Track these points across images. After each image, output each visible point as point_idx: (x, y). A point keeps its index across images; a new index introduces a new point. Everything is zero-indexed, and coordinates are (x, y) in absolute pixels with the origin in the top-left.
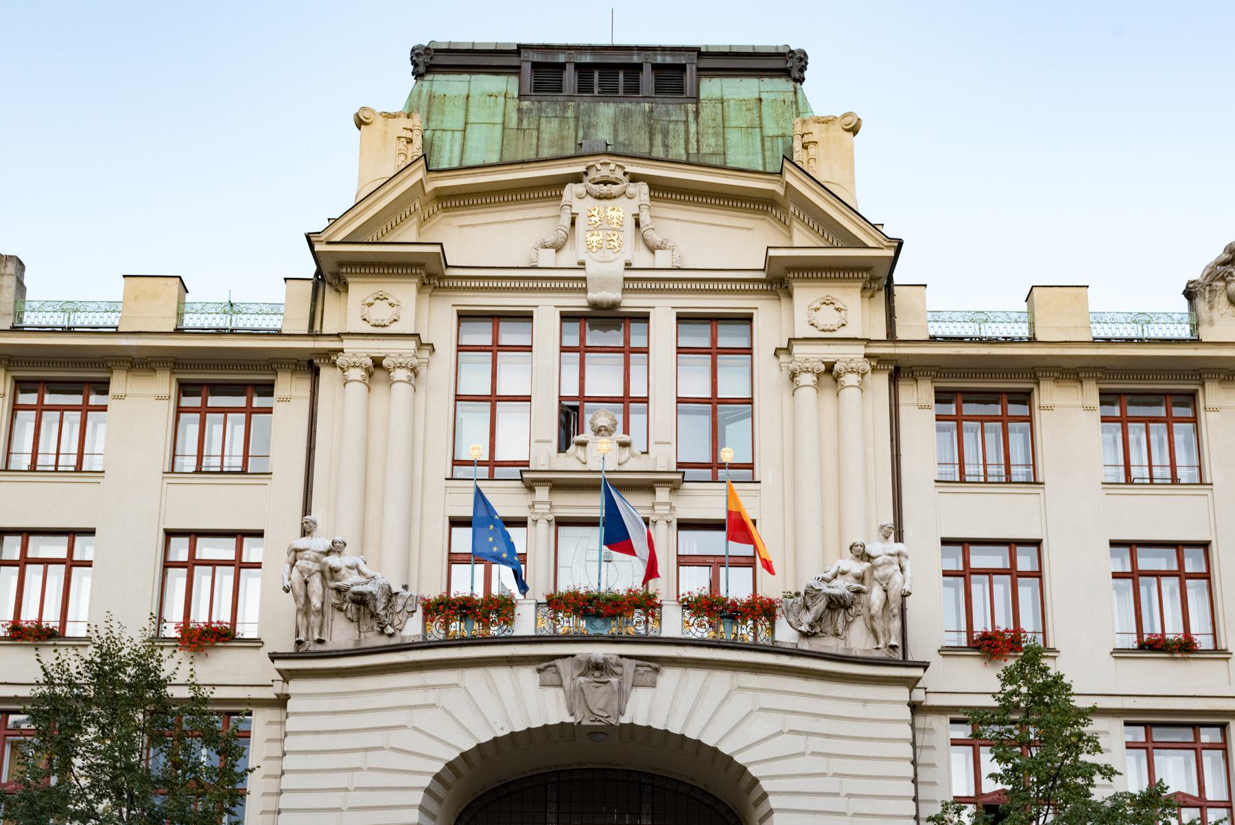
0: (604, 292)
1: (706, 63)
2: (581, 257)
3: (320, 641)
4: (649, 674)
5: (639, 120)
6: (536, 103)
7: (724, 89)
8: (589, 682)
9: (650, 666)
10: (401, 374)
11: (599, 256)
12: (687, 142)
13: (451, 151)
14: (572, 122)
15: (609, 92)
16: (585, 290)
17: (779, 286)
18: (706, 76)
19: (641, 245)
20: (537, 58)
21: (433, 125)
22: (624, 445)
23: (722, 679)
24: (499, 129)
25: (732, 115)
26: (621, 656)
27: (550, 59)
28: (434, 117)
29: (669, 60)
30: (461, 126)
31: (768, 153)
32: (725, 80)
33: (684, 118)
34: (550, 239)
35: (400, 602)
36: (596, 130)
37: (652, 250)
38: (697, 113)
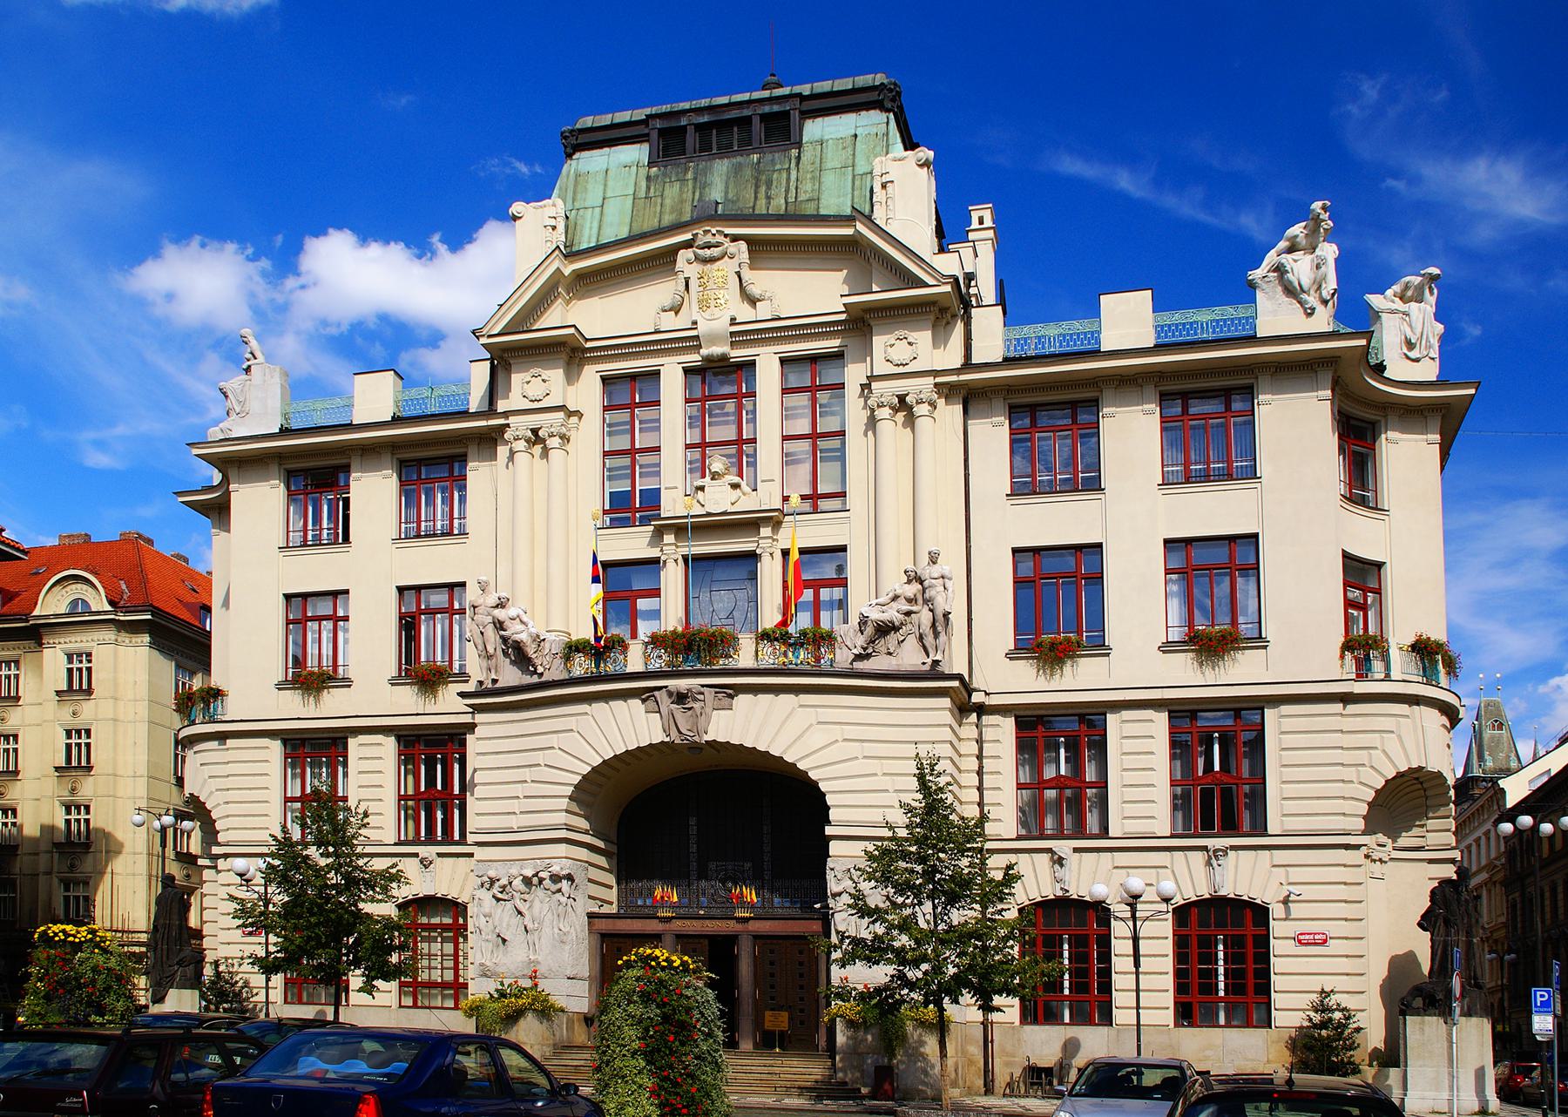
0: (714, 348)
1: (807, 106)
5: (748, 172)
6: (662, 168)
7: (826, 129)
11: (706, 315)
12: (787, 191)
13: (591, 228)
14: (690, 183)
15: (725, 151)
18: (809, 118)
21: (577, 205)
24: (630, 200)
25: (829, 155)
26: (703, 686)
27: (674, 124)
28: (579, 196)
29: (776, 108)
30: (600, 202)
31: (856, 193)
32: (826, 119)
33: (787, 166)
34: (667, 303)
36: (710, 189)
37: (753, 301)
38: (799, 158)
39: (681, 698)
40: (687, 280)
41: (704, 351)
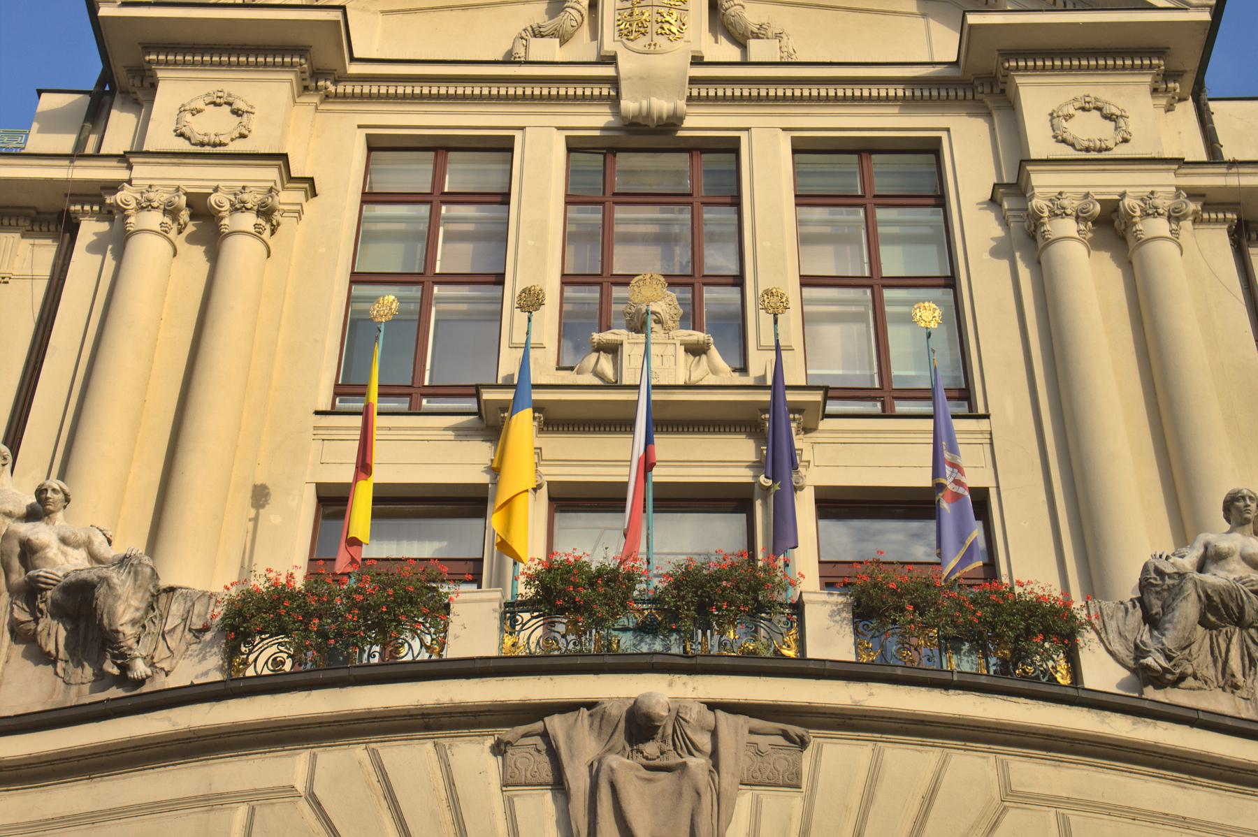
2: (609, 46)
4: (783, 754)
8: (631, 768)
9: (785, 735)
10: (248, 221)
11: (641, 43)
16: (615, 101)
17: (987, 90)
19: (722, 39)
26: (712, 706)
34: (549, 25)
35: (177, 609)
37: (740, 41)
41: (629, 105)
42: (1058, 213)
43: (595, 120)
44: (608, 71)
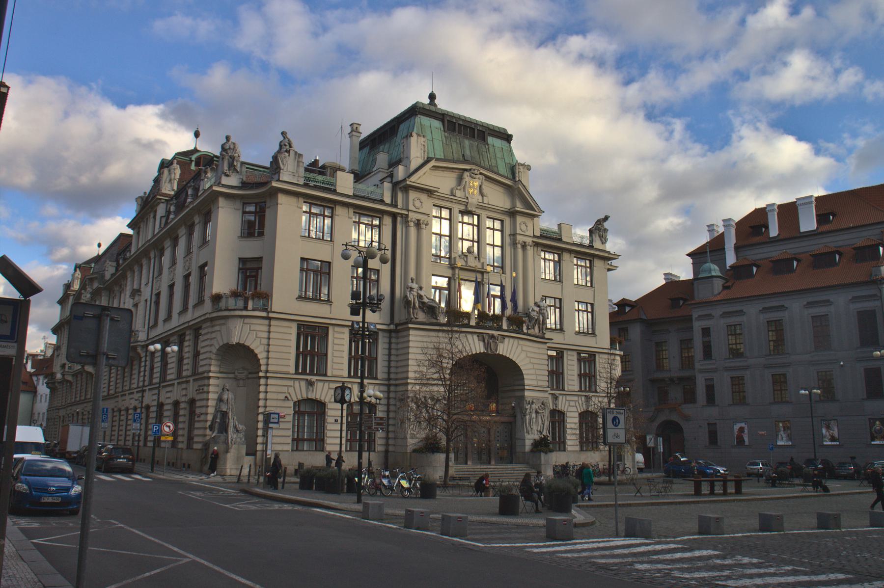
2: (467, 195)
3: (416, 318)
5: (475, 148)
15: (465, 135)
16: (466, 206)
20: (448, 118)
22: (475, 258)
23: (516, 341)
29: (481, 129)
38: (488, 149)
39: (493, 336)
40: (466, 182)
42: (519, 243)
43: (463, 208)
44: (467, 201)
